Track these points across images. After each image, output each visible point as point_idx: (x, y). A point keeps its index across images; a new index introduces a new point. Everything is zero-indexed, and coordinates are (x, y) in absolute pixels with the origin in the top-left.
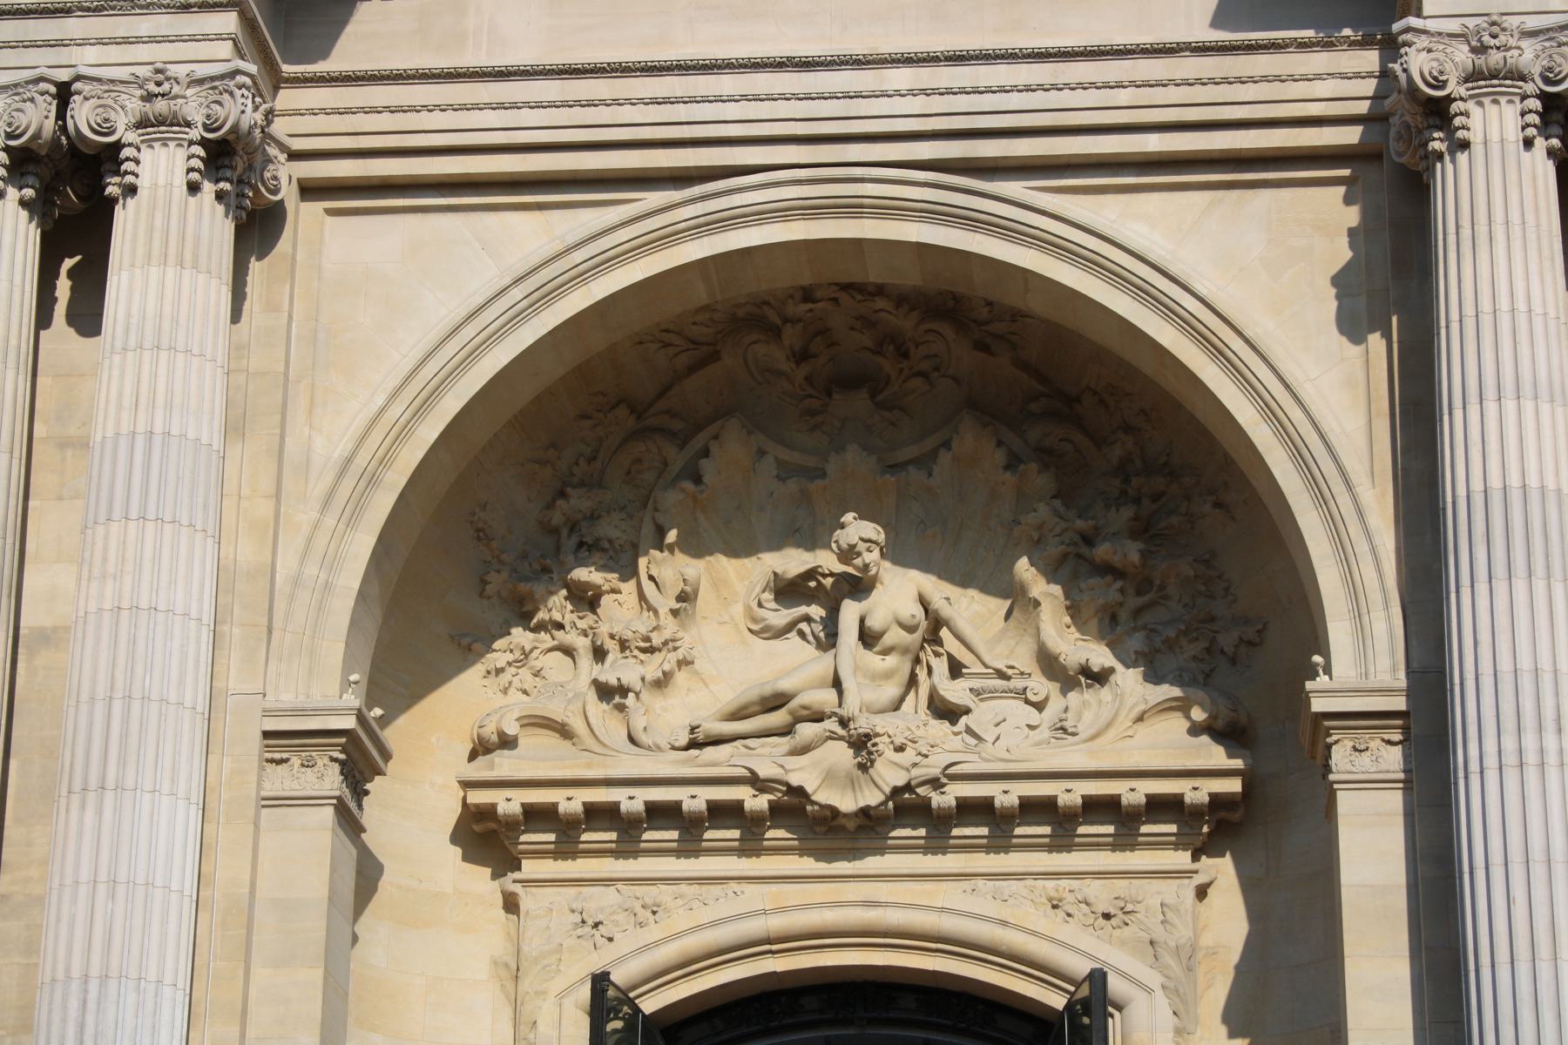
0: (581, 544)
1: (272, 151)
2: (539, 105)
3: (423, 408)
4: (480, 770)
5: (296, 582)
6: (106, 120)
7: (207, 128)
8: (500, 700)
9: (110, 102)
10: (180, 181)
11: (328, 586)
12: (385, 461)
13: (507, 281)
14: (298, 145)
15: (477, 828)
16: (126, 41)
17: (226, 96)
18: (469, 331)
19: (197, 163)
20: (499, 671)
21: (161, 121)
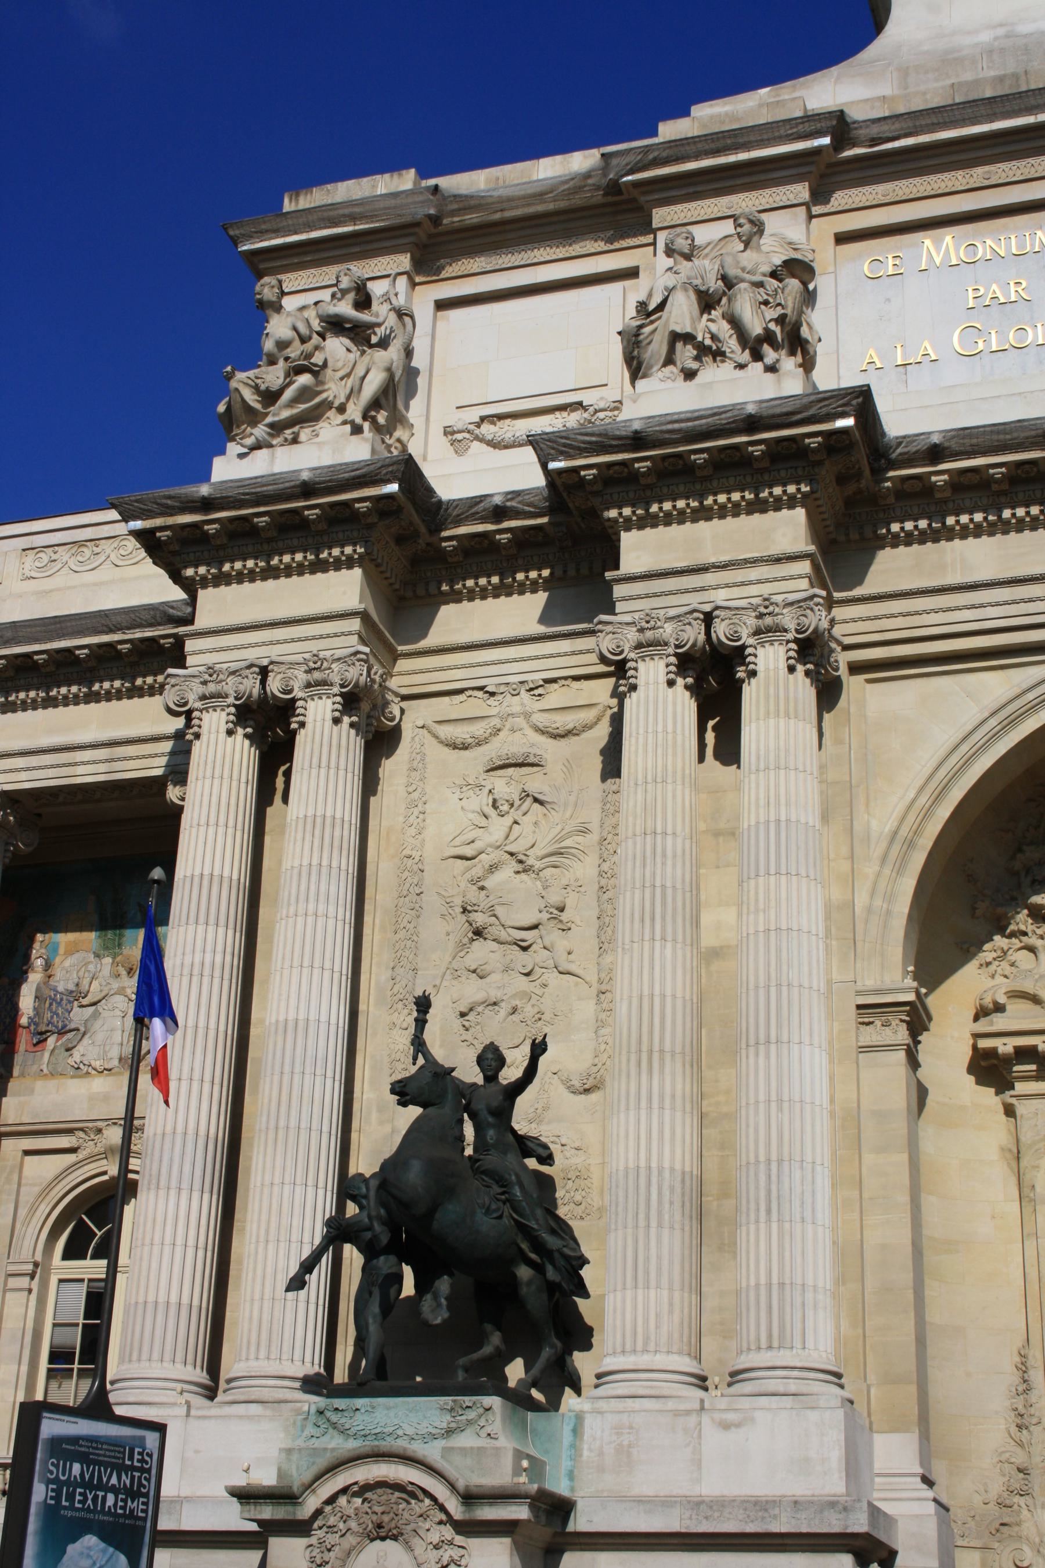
0: (1034, 882)
1: (833, 645)
2: (998, 604)
3: (939, 797)
4: (982, 1026)
5: (869, 910)
6: (736, 632)
7: (798, 631)
8: (991, 983)
9: (737, 621)
10: (783, 666)
11: (888, 912)
12: (917, 832)
13: (986, 714)
14: (848, 641)
15: (983, 1063)
16: (743, 584)
17: (808, 612)
18: (964, 748)
19: (792, 654)
20: (988, 964)
21: (769, 630)
